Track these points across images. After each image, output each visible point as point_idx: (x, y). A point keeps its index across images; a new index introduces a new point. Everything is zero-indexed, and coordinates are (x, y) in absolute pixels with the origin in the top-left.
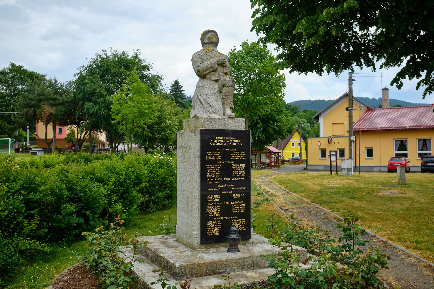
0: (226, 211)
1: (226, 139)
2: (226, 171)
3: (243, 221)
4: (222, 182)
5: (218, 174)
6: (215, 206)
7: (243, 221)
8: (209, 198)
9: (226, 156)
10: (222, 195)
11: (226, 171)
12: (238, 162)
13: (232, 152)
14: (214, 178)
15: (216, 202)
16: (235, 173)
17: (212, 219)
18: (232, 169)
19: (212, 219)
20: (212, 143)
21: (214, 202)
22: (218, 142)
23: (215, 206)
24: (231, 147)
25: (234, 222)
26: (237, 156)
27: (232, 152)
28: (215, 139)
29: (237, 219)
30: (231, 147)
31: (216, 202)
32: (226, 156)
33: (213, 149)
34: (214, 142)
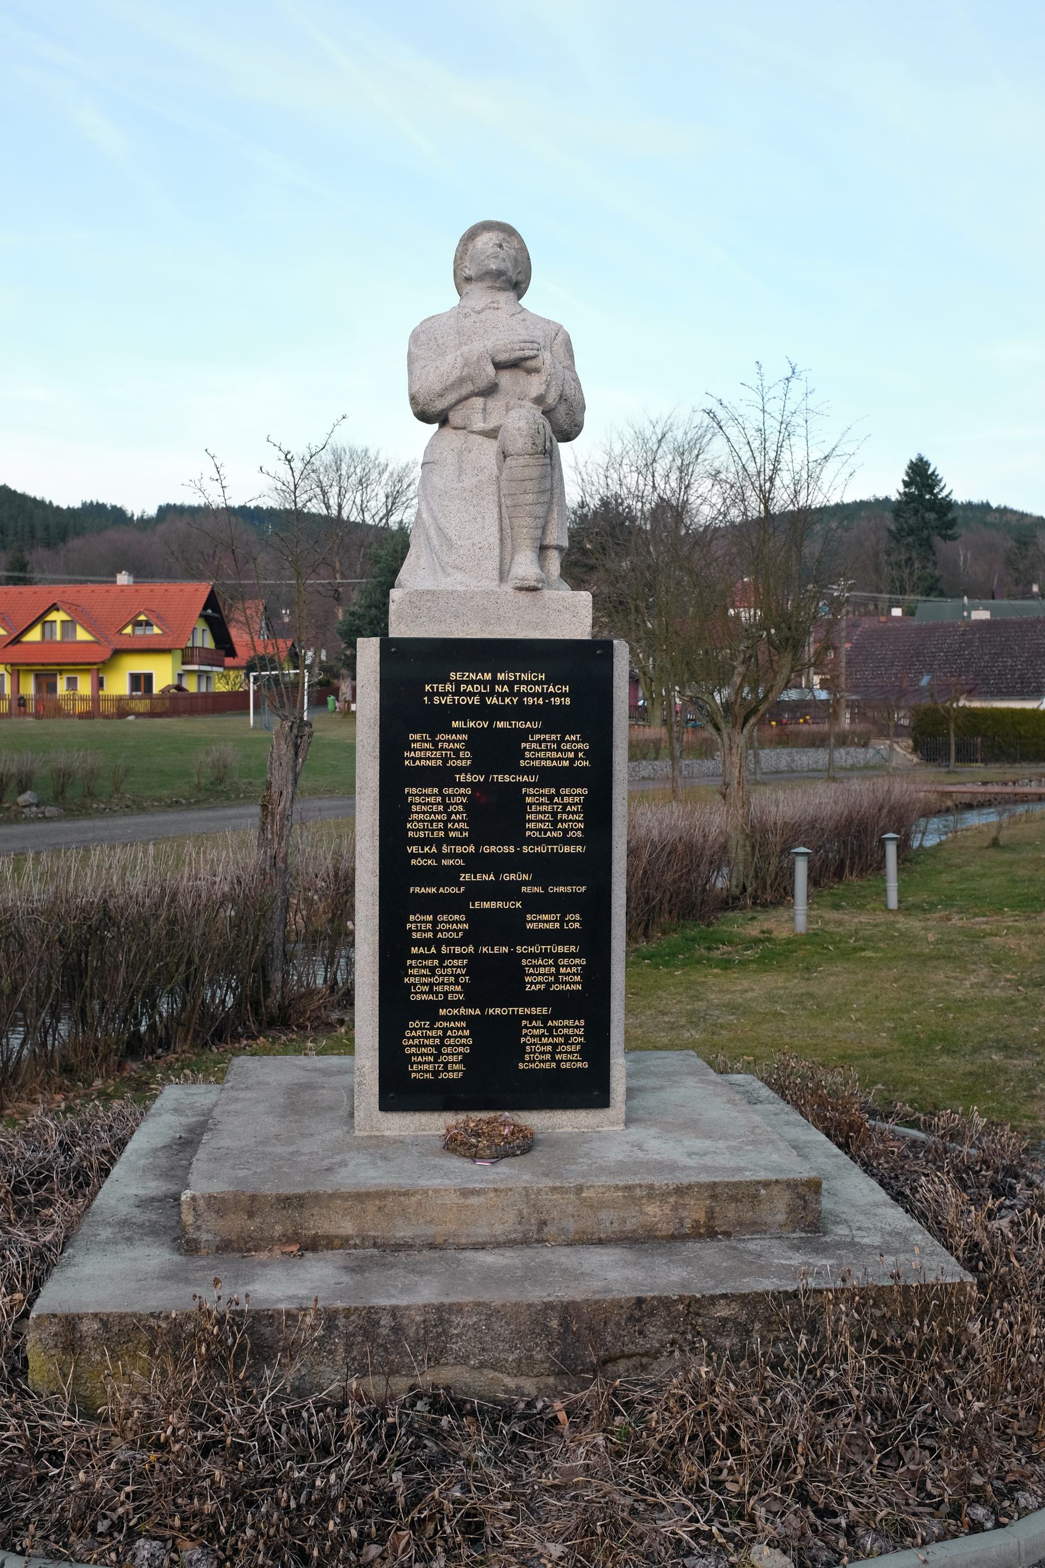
0: (494, 980)
1: (494, 681)
2: (496, 814)
3: (574, 1028)
4: (475, 863)
5: (460, 827)
6: (442, 958)
7: (574, 1028)
8: (419, 924)
9: (495, 750)
10: (473, 917)
11: (496, 814)
12: (550, 777)
13: (524, 735)
14: (439, 842)
15: (449, 942)
16: (536, 823)
17: (429, 1012)
18: (522, 808)
19: (429, 1012)
20: (431, 695)
21: (438, 943)
22: (458, 693)
23: (442, 958)
24: (521, 711)
25: (532, 1035)
26: (544, 751)
27: (524, 735)
28: (446, 680)
29: (545, 1019)
30: (521, 711)
31: (449, 942)
32: (495, 750)
33: (437, 721)
34: (441, 694)
